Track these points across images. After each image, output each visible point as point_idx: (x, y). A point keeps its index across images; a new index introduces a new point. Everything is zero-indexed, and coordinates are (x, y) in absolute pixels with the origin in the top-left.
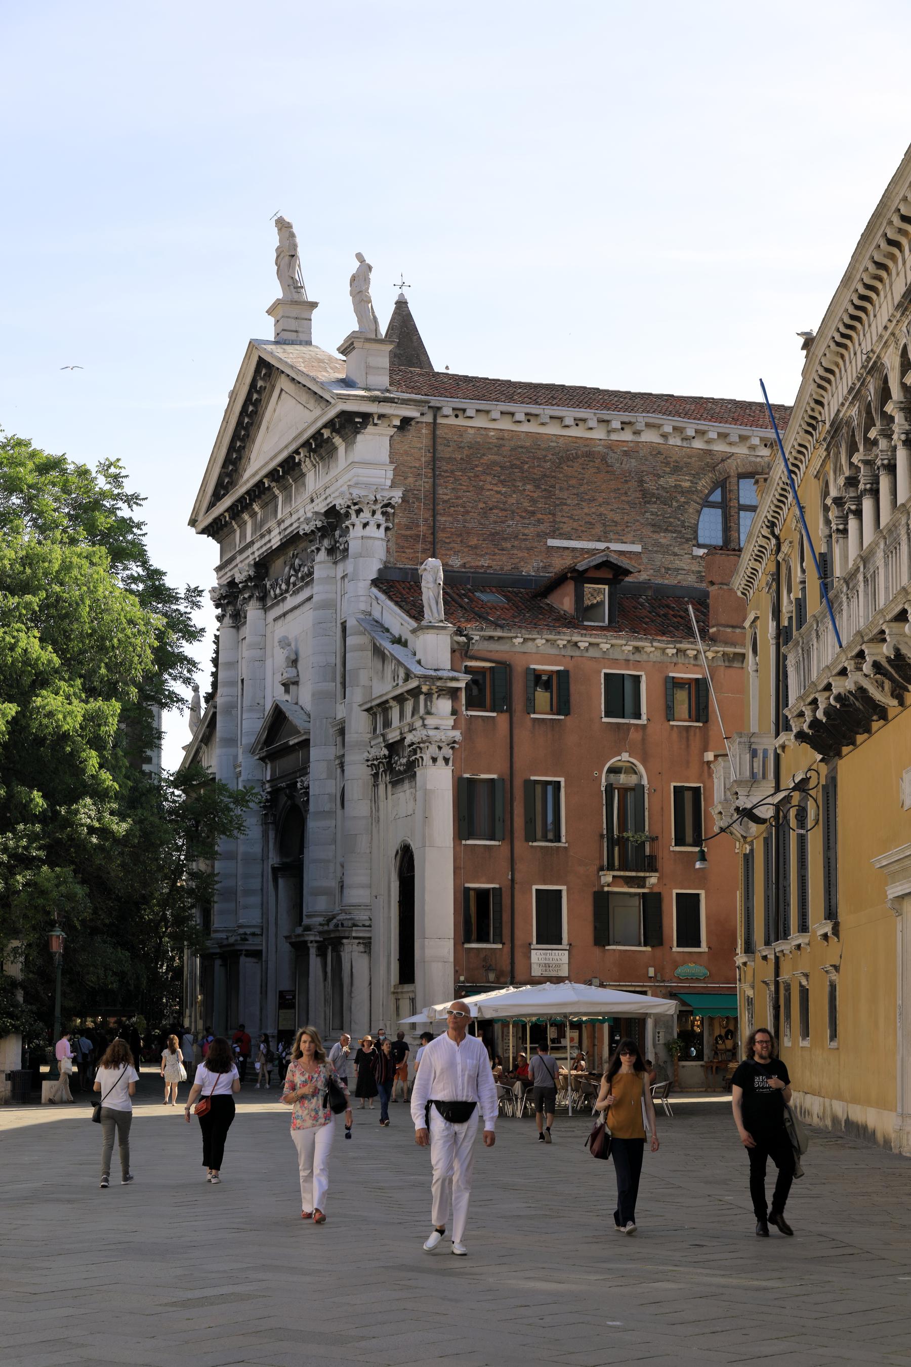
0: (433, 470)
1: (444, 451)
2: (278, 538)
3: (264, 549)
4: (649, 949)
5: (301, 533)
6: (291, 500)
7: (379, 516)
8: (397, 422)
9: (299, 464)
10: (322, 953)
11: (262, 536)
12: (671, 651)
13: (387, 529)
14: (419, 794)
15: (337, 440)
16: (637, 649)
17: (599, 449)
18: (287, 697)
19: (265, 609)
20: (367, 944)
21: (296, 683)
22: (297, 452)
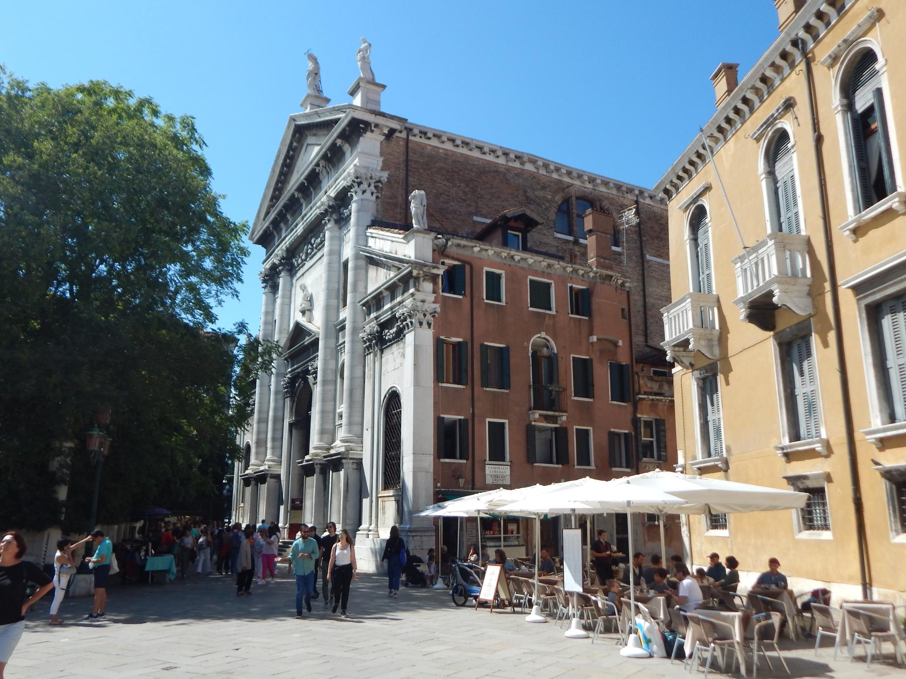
0: (407, 166)
4: (560, 466)
7: (372, 187)
8: (386, 131)
9: (318, 174)
12: (569, 270)
13: (377, 197)
15: (346, 148)
16: (549, 266)
17: (501, 170)
22: (317, 165)
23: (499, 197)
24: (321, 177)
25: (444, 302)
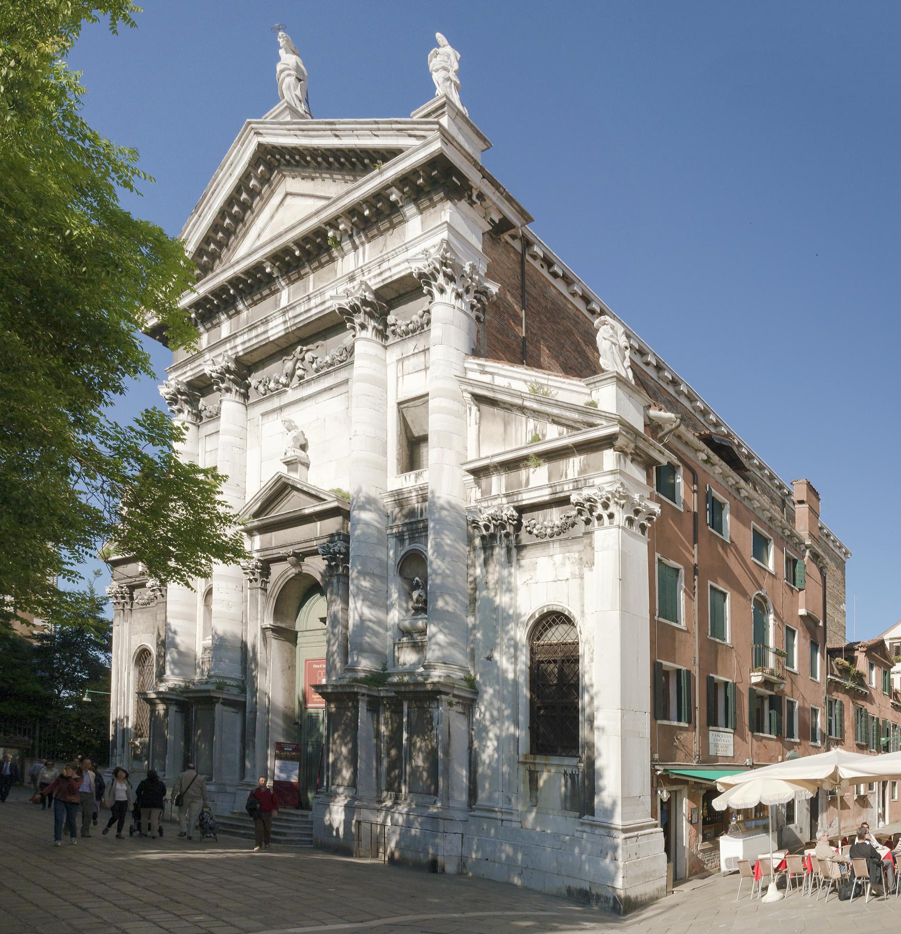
2: (282, 327)
3: (255, 341)
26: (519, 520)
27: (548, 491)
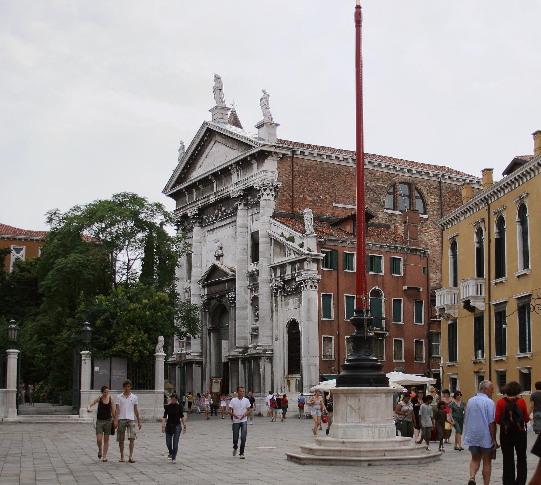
0: (292, 175)
1: (297, 168)
2: (214, 199)
3: (205, 203)
5: (232, 197)
6: (222, 184)
7: (273, 192)
10: (243, 363)
11: (205, 198)
13: (275, 197)
14: (304, 301)
15: (253, 161)
18: (218, 262)
19: (202, 227)
20: (270, 359)
21: (222, 256)
22: (231, 165)
23: (349, 189)
24: (232, 171)
25: (322, 273)
26: (284, 285)
27: (290, 276)
